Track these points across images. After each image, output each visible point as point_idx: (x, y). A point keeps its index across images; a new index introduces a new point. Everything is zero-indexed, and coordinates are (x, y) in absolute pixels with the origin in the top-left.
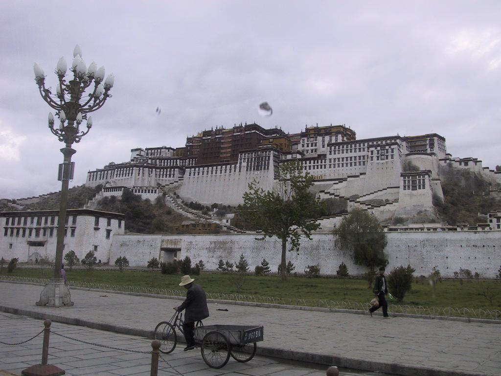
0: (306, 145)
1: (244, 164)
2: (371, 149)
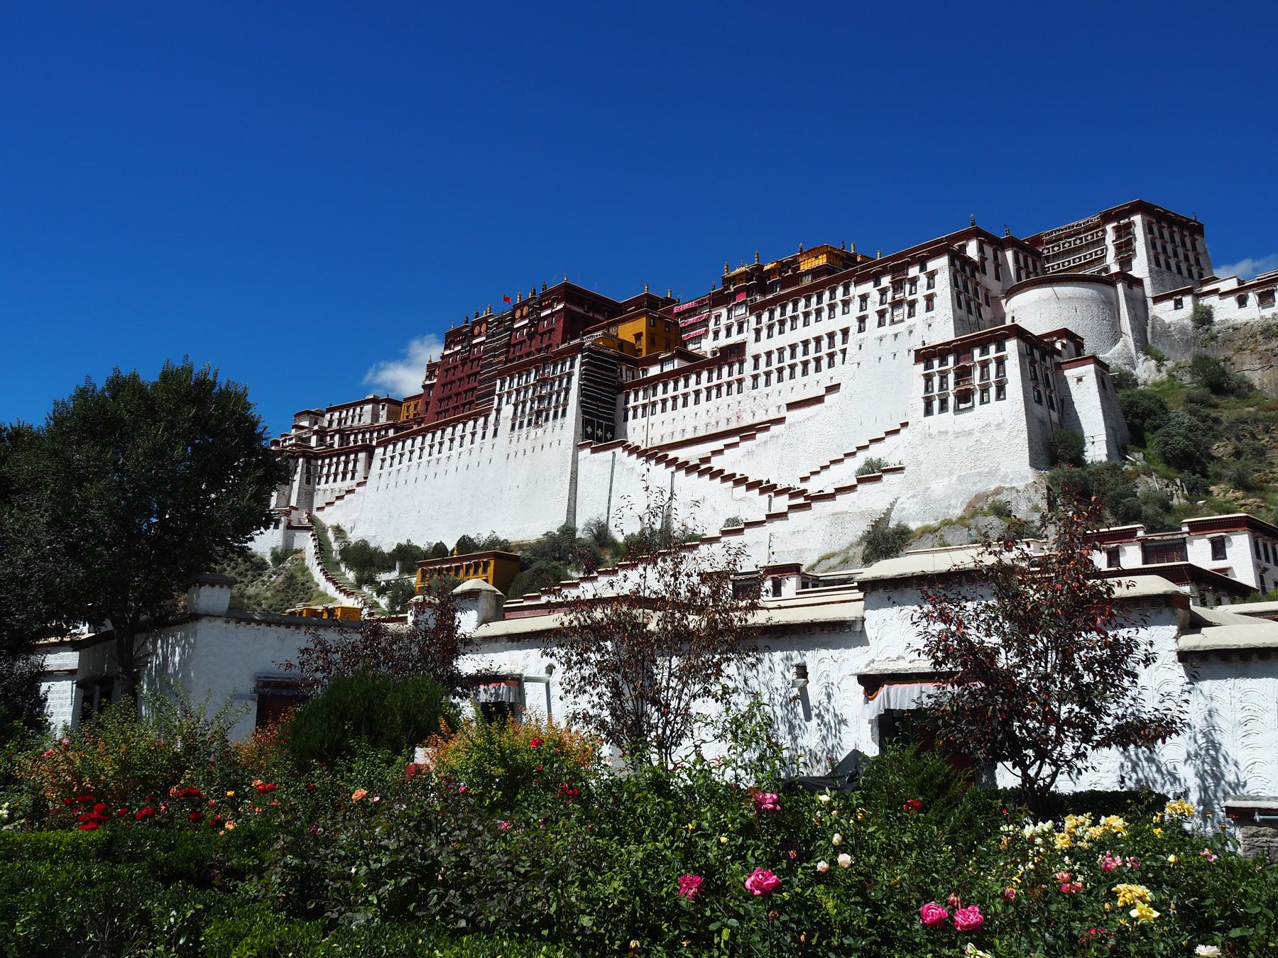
0: (723, 333)
1: (507, 410)
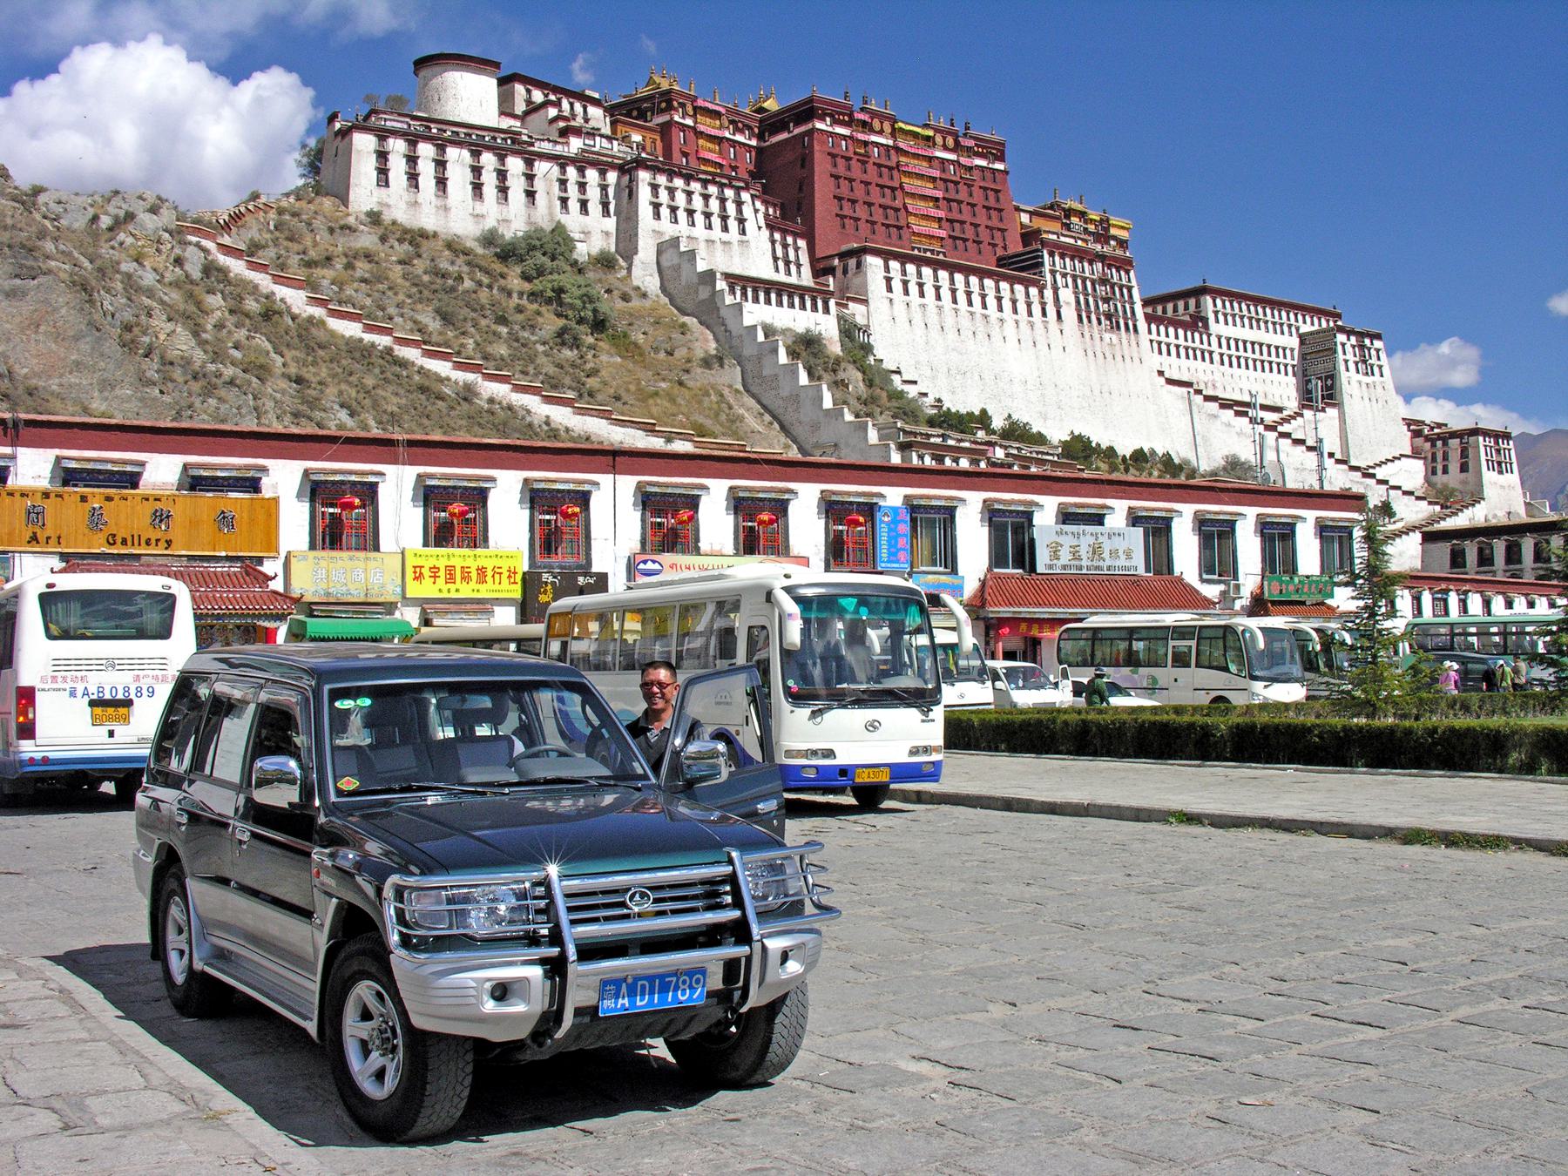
1: (1067, 295)
2: (1341, 338)
